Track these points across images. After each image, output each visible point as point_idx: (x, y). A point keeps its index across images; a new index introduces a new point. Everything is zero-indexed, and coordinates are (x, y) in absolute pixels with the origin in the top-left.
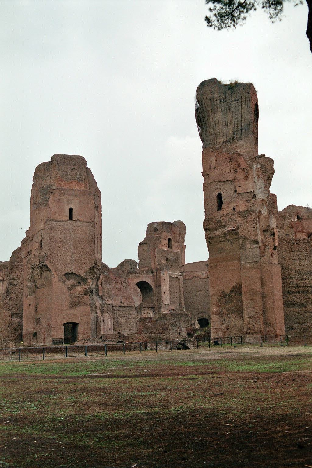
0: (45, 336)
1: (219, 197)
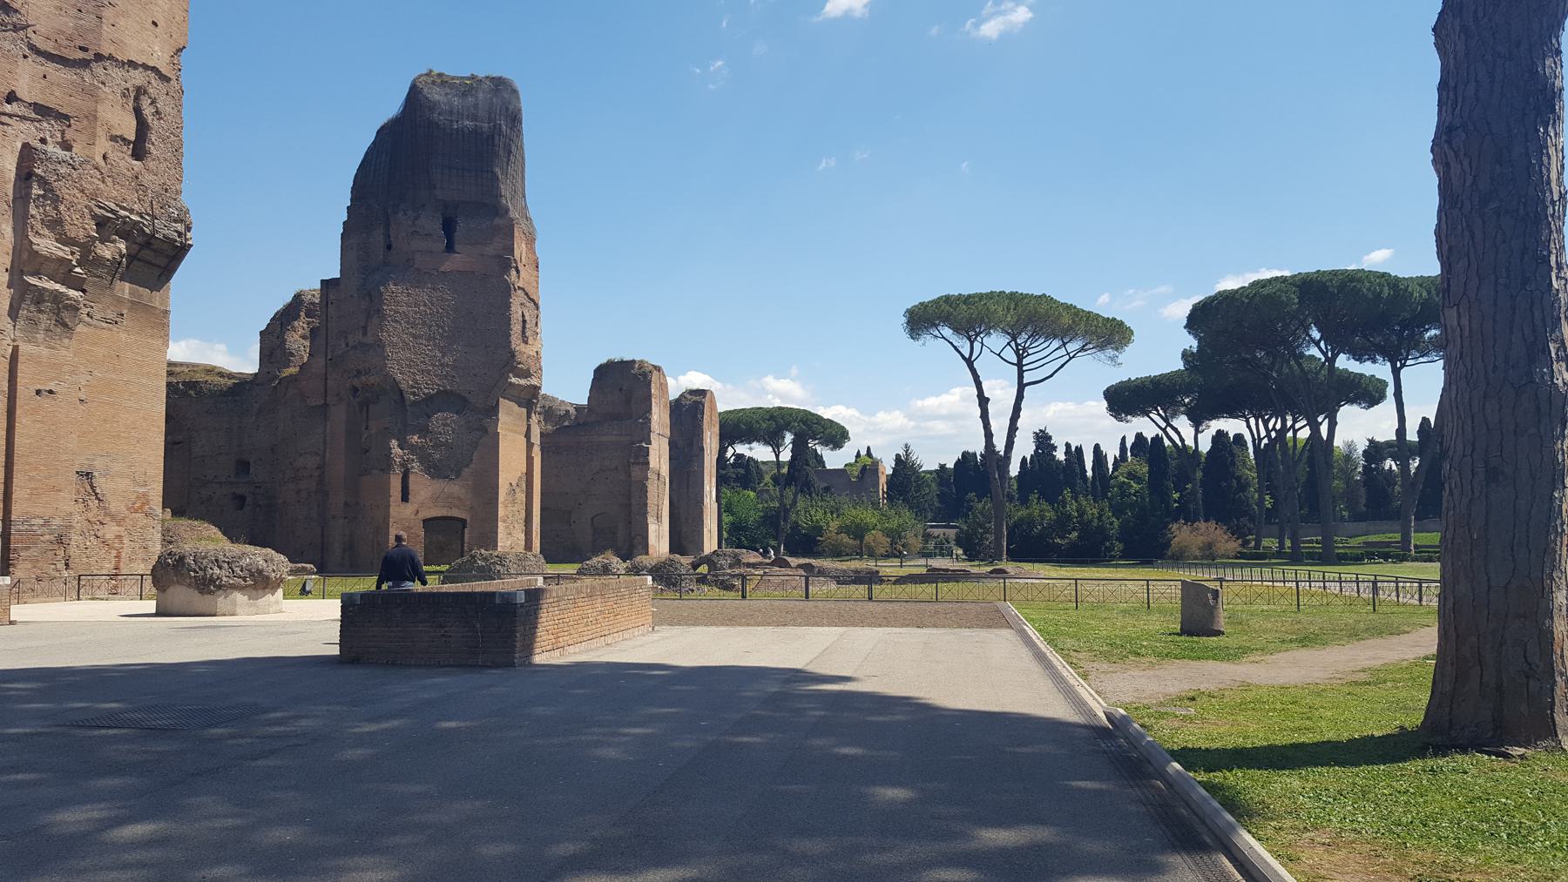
0: (118, 556)
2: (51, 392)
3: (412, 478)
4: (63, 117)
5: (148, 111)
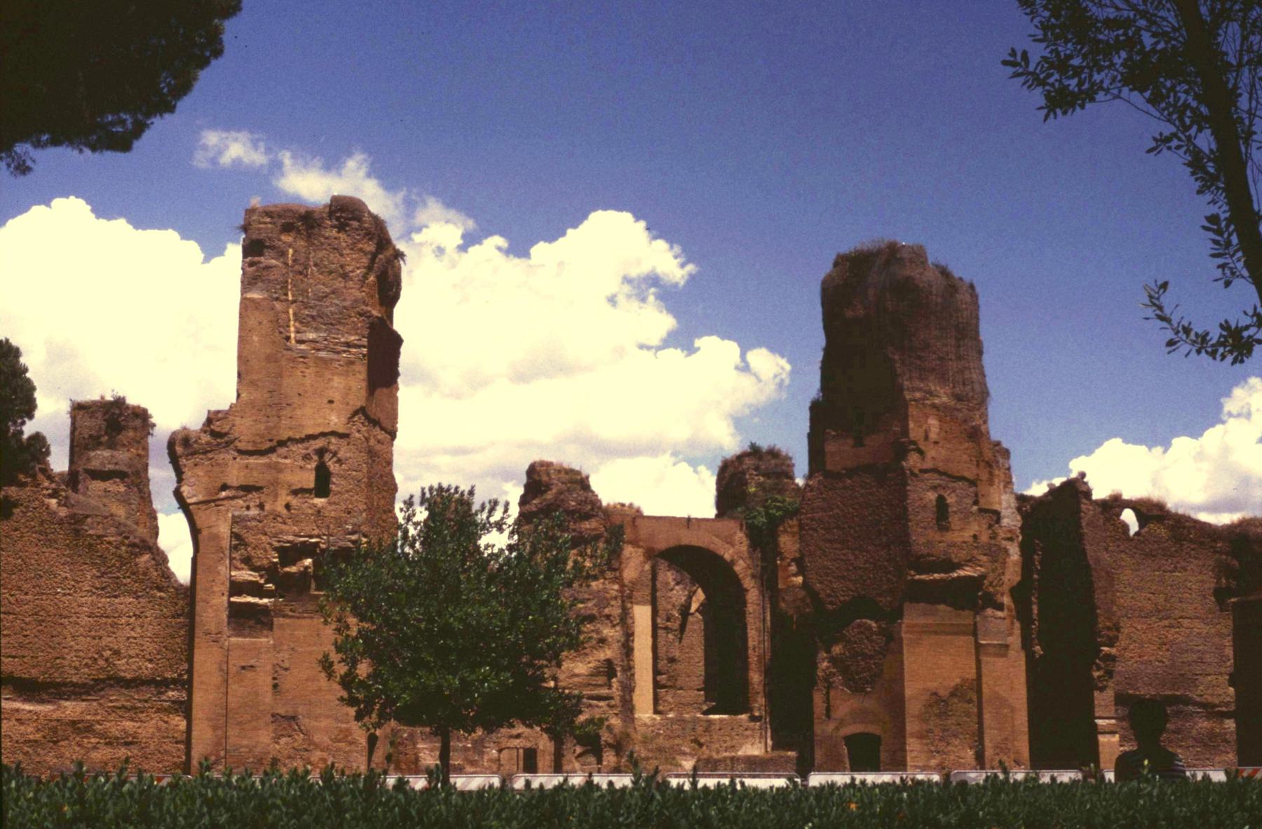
2: (252, 666)
4: (258, 489)
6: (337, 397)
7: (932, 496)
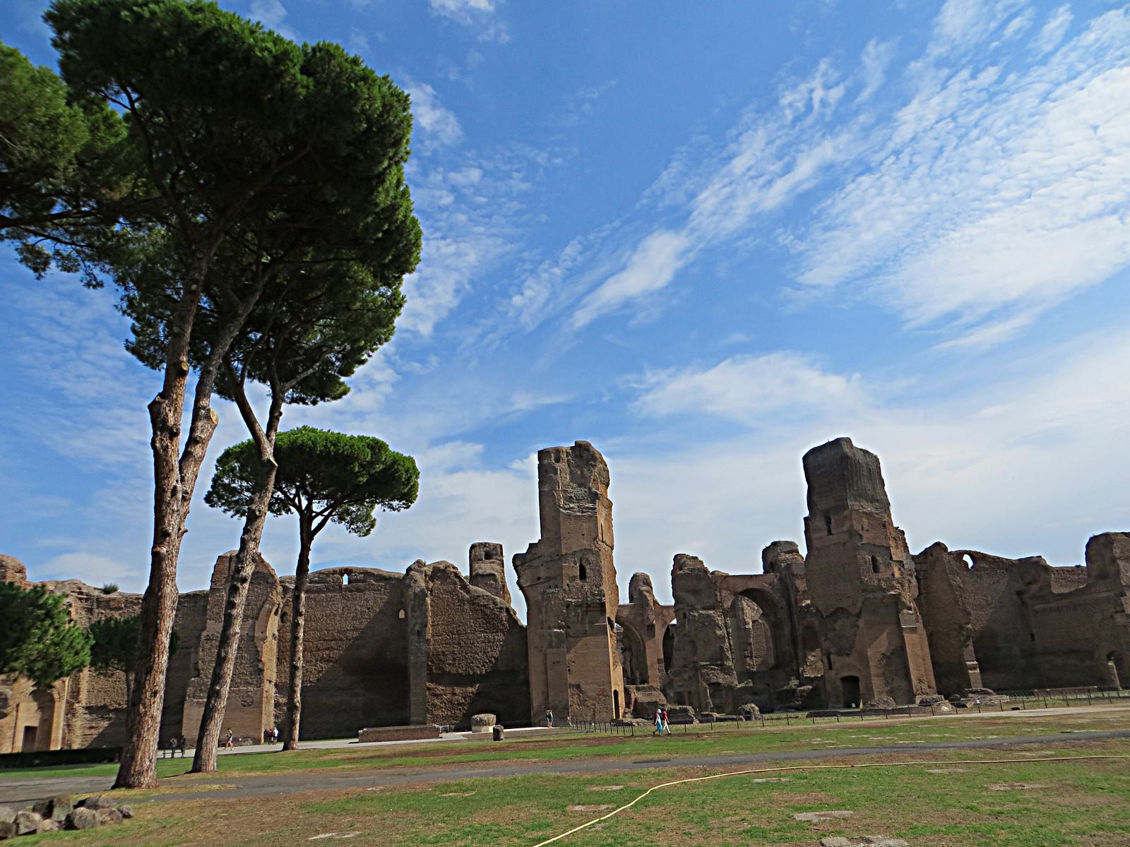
0: (594, 711)
1: (874, 559)
3: (832, 656)
5: (584, 564)
6: (585, 532)
7: (869, 558)
